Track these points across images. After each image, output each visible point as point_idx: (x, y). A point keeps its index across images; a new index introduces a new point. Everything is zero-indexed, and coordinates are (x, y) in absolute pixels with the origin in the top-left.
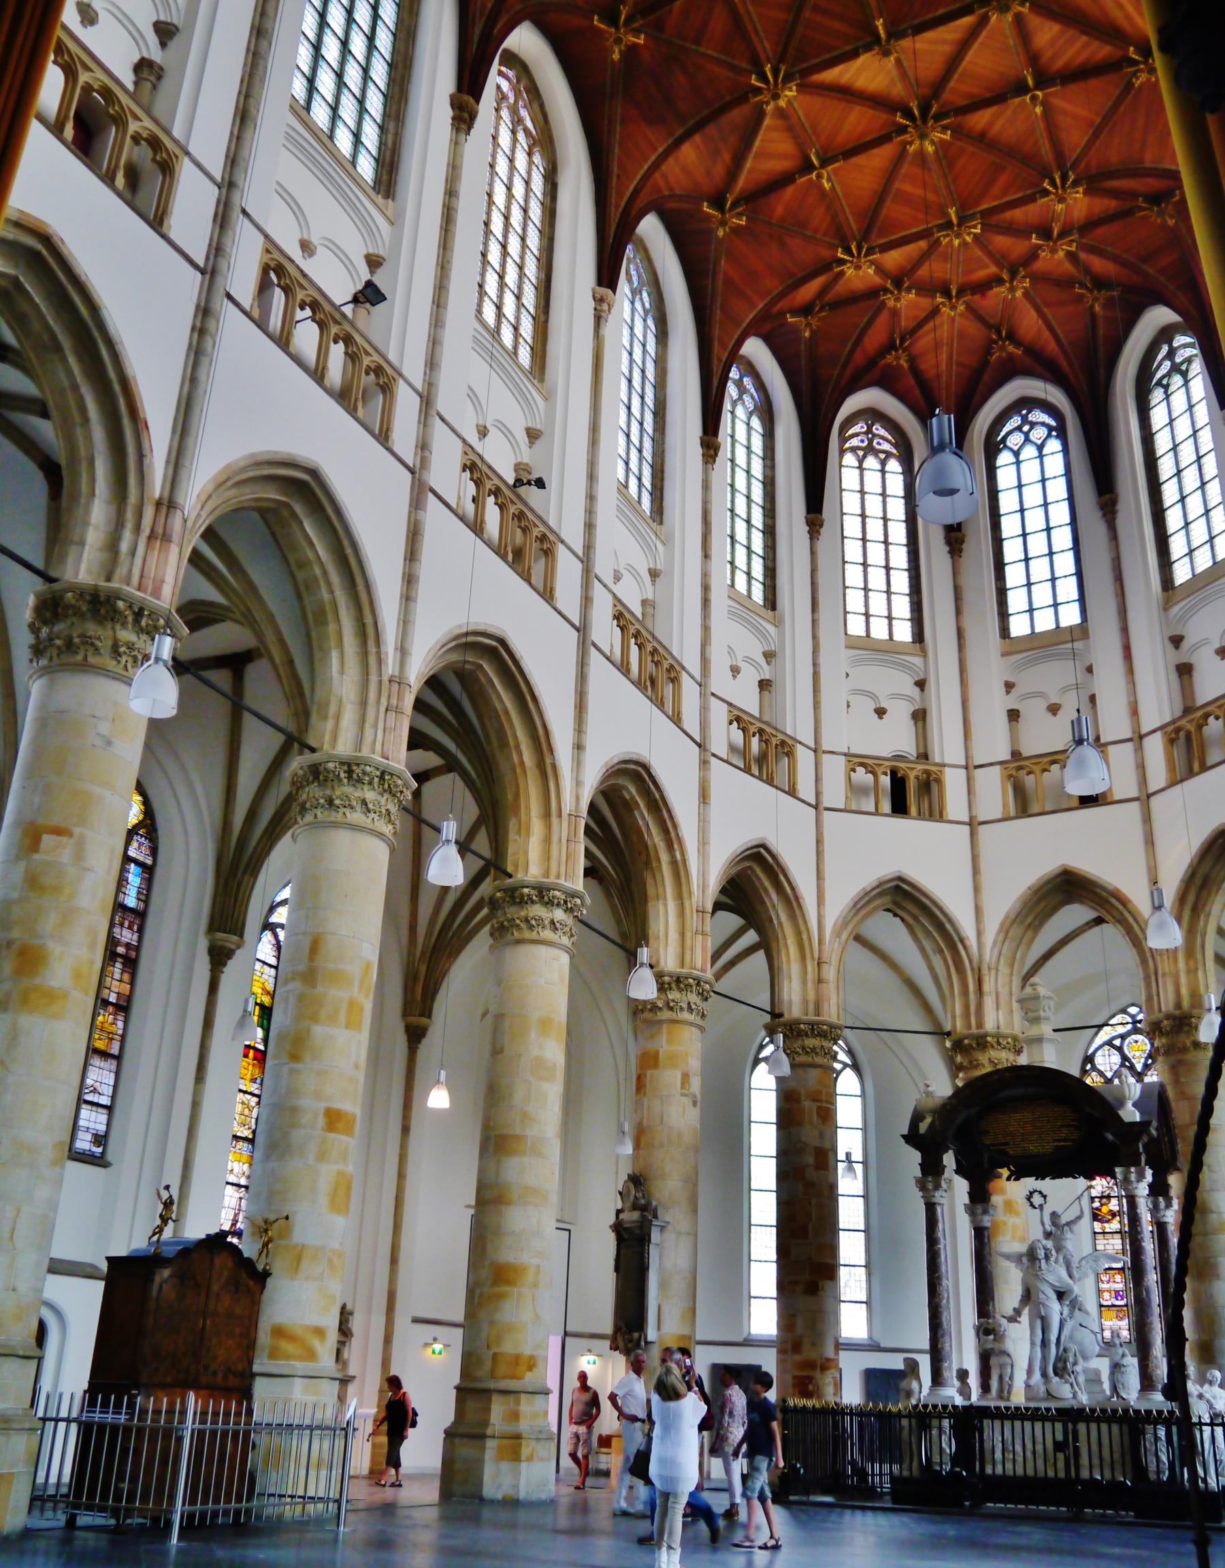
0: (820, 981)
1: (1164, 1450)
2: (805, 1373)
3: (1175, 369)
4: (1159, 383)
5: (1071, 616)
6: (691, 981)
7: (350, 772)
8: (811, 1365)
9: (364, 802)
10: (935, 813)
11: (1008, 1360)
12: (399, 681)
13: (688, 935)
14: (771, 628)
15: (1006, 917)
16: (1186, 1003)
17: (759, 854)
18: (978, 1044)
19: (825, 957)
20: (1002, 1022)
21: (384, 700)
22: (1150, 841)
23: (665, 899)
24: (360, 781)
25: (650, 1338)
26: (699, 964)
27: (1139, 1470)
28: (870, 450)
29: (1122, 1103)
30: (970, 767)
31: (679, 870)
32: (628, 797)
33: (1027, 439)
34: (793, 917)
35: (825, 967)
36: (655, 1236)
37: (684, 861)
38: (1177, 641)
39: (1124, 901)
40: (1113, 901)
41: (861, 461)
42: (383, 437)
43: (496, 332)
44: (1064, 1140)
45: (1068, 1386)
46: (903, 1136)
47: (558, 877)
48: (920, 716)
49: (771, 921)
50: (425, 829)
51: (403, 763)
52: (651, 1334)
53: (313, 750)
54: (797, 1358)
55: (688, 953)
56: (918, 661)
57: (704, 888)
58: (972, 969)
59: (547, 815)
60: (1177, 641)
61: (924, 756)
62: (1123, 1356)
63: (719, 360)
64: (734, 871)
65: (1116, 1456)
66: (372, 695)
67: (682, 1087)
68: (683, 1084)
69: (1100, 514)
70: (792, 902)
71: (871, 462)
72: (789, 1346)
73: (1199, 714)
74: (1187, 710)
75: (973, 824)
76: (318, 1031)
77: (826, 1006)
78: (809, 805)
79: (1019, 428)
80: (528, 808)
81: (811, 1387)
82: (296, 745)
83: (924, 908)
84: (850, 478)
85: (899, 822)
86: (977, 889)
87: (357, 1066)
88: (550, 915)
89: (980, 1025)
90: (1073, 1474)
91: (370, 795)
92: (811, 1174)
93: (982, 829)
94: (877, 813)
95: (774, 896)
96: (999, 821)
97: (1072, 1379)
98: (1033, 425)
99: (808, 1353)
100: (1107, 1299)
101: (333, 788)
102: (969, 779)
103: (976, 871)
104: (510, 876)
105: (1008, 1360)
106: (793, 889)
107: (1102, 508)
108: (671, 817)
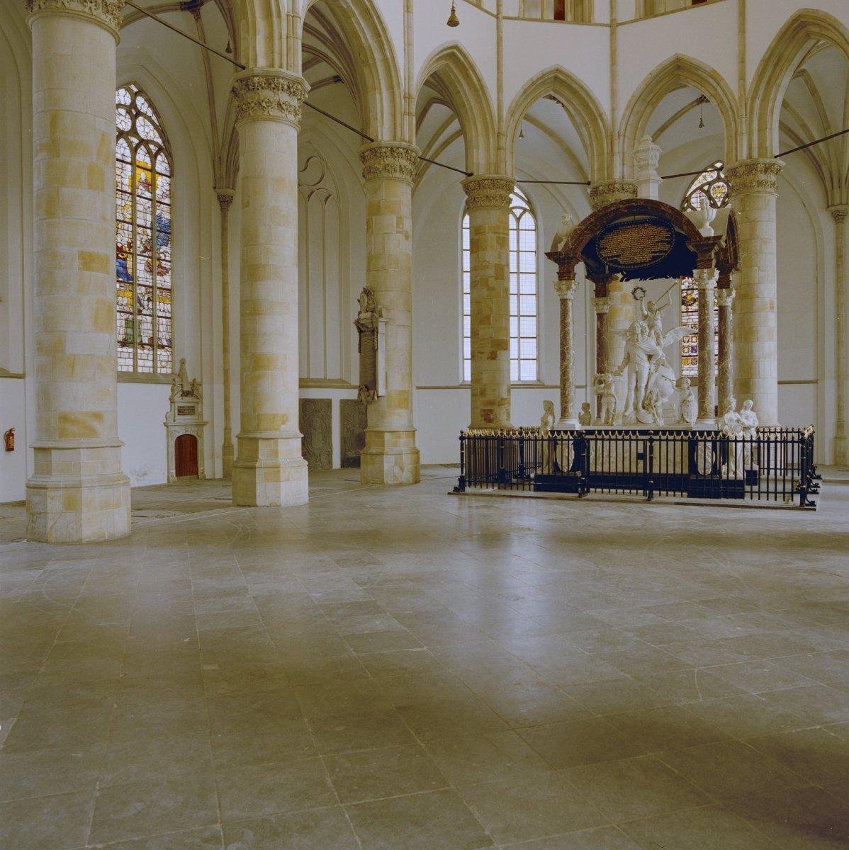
0: (499, 148)
1: (710, 455)
2: (486, 408)
6: (401, 150)
8: (492, 403)
11: (613, 399)
13: (398, 116)
15: (633, 97)
17: (453, 53)
18: (609, 190)
19: (503, 130)
20: (625, 174)
22: (742, 30)
25: (380, 394)
26: (407, 139)
27: (693, 465)
29: (702, 225)
31: (389, 64)
32: (345, 6)
34: (479, 102)
35: (503, 139)
36: (381, 328)
37: (393, 58)
40: (711, 81)
44: (660, 252)
45: (651, 415)
46: (547, 254)
47: (281, 66)
49: (464, 106)
52: (381, 391)
54: (484, 399)
55: (398, 129)
57: (409, 78)
58: (607, 136)
59: (268, 16)
62: (689, 395)
64: (434, 68)
65: (678, 459)
67: (398, 226)
68: (398, 224)
70: (479, 90)
72: (478, 392)
75: (613, 25)
77: (503, 165)
78: (492, 15)
81: (492, 416)
83: (575, 92)
85: (559, 26)
86: (613, 76)
88: (277, 98)
89: (610, 176)
90: (648, 471)
92: (492, 282)
93: (620, 29)
94: (542, 20)
95: (466, 87)
96: (632, 22)
97: (654, 411)
99: (490, 396)
103: (613, 62)
105: (613, 399)
106: (479, 80)
108: (381, 23)
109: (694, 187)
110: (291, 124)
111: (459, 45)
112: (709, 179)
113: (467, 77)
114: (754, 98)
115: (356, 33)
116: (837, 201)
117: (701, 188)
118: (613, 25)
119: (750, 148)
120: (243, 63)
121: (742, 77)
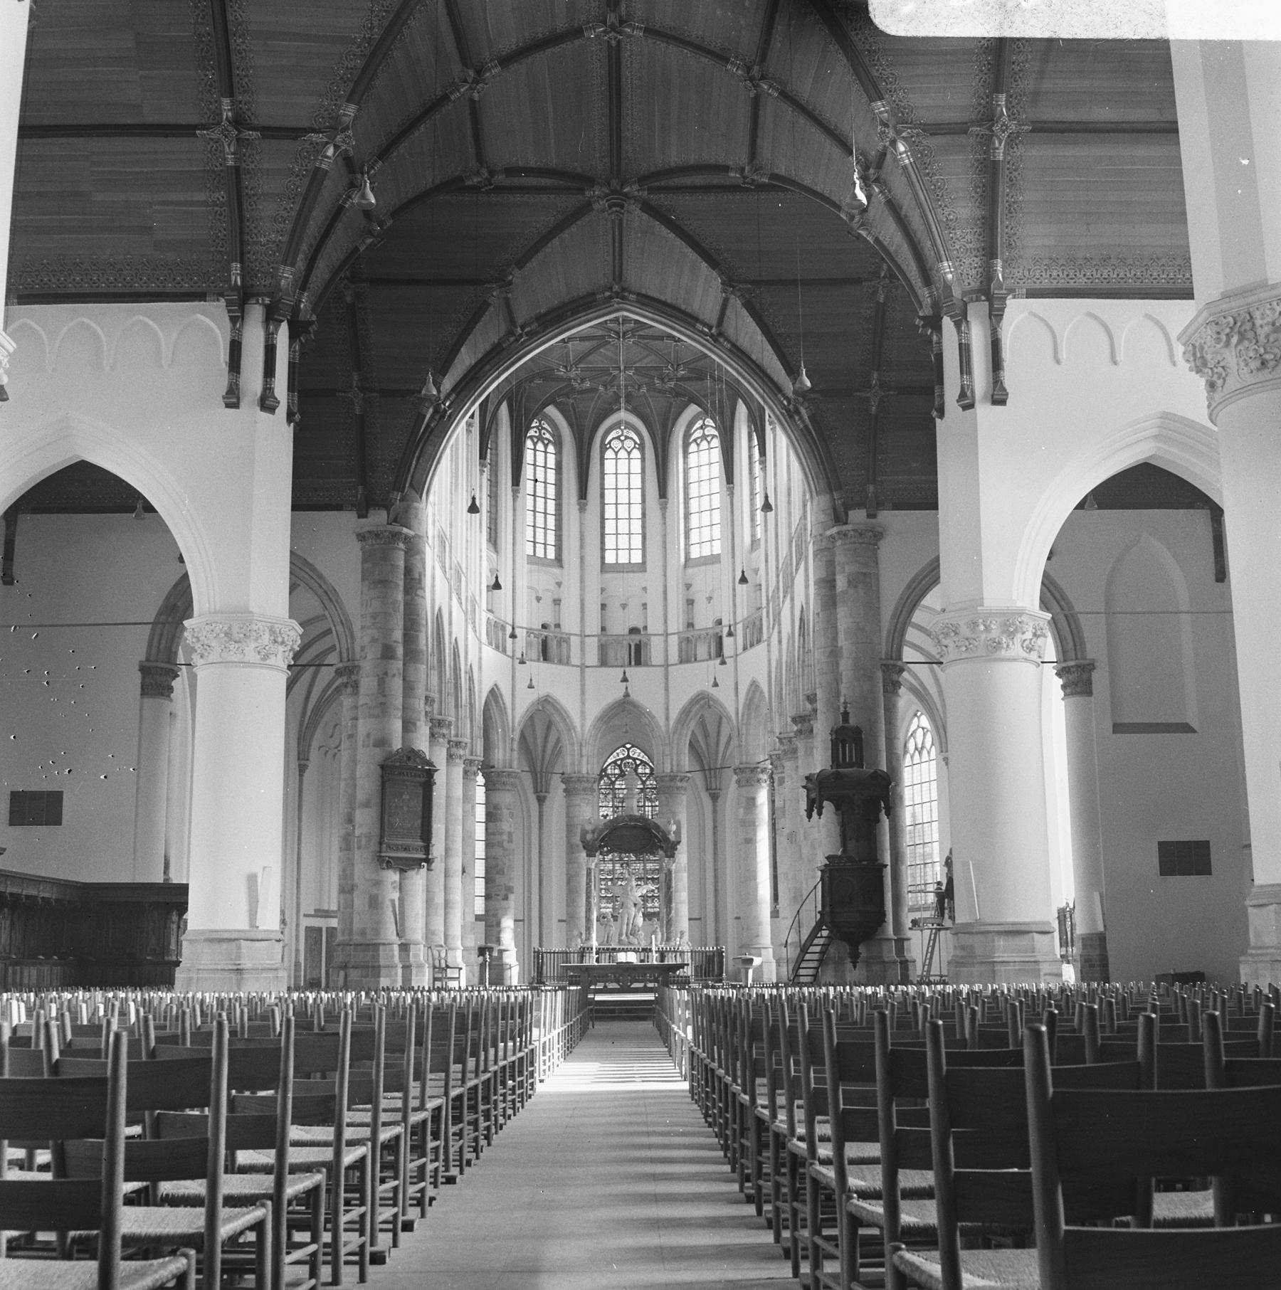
0: (512, 750)
3: (704, 437)
4: (695, 440)
5: (637, 558)
7: (439, 724)
10: (564, 661)
14: (494, 556)
16: (675, 769)
28: (540, 438)
30: (583, 636)
33: (623, 447)
38: (688, 586)
39: (653, 717)
41: (535, 444)
48: (557, 602)
56: (557, 571)
60: (688, 586)
61: (558, 626)
69: (659, 507)
70: (502, 711)
71: (540, 446)
73: (698, 633)
74: (690, 625)
75: (583, 667)
79: (618, 438)
84: (529, 456)
85: (544, 666)
86: (583, 703)
92: (506, 844)
94: (538, 660)
98: (627, 438)
100: (603, 893)
102: (582, 643)
107: (661, 504)
109: (609, 761)
112: (621, 756)
113: (497, 702)
114: (674, 733)
116: (714, 787)
117: (615, 762)
118: (583, 667)
119: (672, 765)
121: (667, 719)
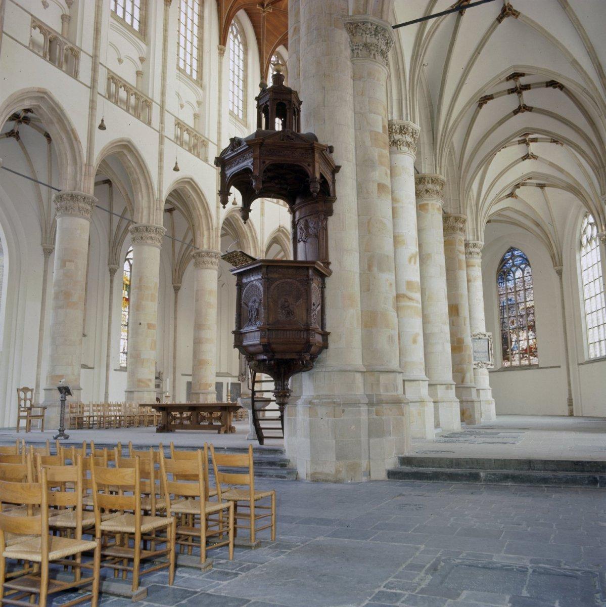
7: (147, 229)
9: (151, 238)
12: (160, 200)
21: (155, 206)
23: (250, 248)
24: (150, 231)
32: (236, 217)
42: (149, 123)
43: (184, 70)
47: (212, 248)
50: (171, 235)
51: (162, 225)
53: (136, 223)
57: (262, 243)
59: (208, 229)
63: (266, 58)
66: (152, 205)
76: (143, 303)
80: (203, 228)
82: (131, 222)
87: (155, 312)
91: (153, 235)
101: (142, 234)
104: (198, 249)
110: (215, 269)
111: (284, 226)
115: (241, 227)
120: (198, 247)
